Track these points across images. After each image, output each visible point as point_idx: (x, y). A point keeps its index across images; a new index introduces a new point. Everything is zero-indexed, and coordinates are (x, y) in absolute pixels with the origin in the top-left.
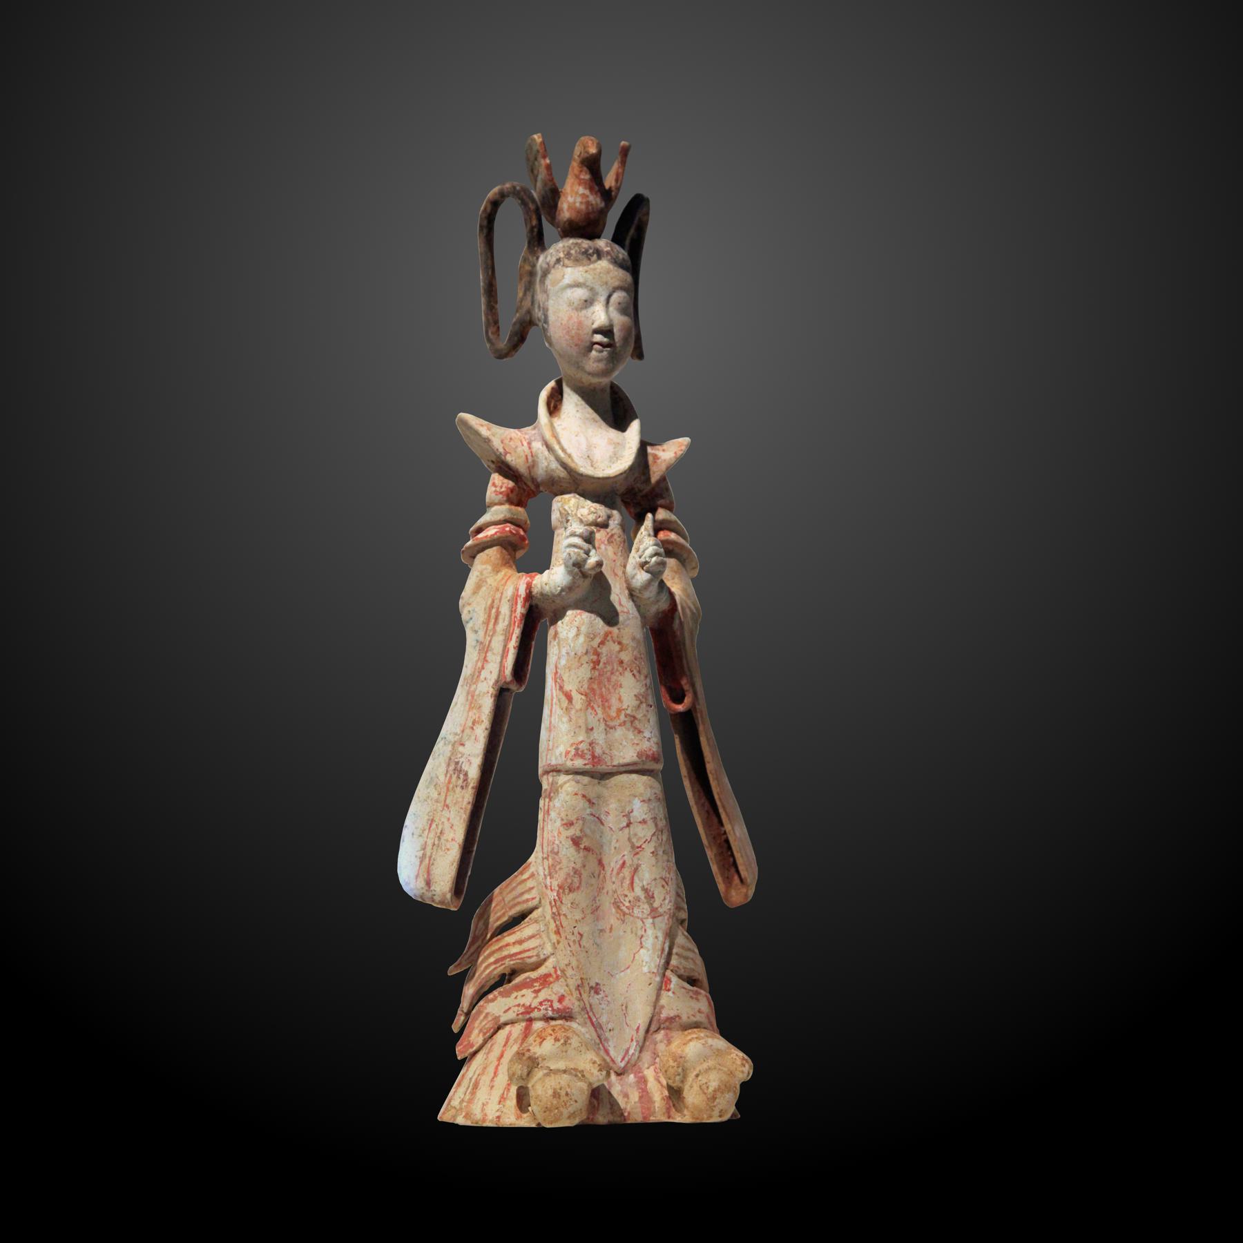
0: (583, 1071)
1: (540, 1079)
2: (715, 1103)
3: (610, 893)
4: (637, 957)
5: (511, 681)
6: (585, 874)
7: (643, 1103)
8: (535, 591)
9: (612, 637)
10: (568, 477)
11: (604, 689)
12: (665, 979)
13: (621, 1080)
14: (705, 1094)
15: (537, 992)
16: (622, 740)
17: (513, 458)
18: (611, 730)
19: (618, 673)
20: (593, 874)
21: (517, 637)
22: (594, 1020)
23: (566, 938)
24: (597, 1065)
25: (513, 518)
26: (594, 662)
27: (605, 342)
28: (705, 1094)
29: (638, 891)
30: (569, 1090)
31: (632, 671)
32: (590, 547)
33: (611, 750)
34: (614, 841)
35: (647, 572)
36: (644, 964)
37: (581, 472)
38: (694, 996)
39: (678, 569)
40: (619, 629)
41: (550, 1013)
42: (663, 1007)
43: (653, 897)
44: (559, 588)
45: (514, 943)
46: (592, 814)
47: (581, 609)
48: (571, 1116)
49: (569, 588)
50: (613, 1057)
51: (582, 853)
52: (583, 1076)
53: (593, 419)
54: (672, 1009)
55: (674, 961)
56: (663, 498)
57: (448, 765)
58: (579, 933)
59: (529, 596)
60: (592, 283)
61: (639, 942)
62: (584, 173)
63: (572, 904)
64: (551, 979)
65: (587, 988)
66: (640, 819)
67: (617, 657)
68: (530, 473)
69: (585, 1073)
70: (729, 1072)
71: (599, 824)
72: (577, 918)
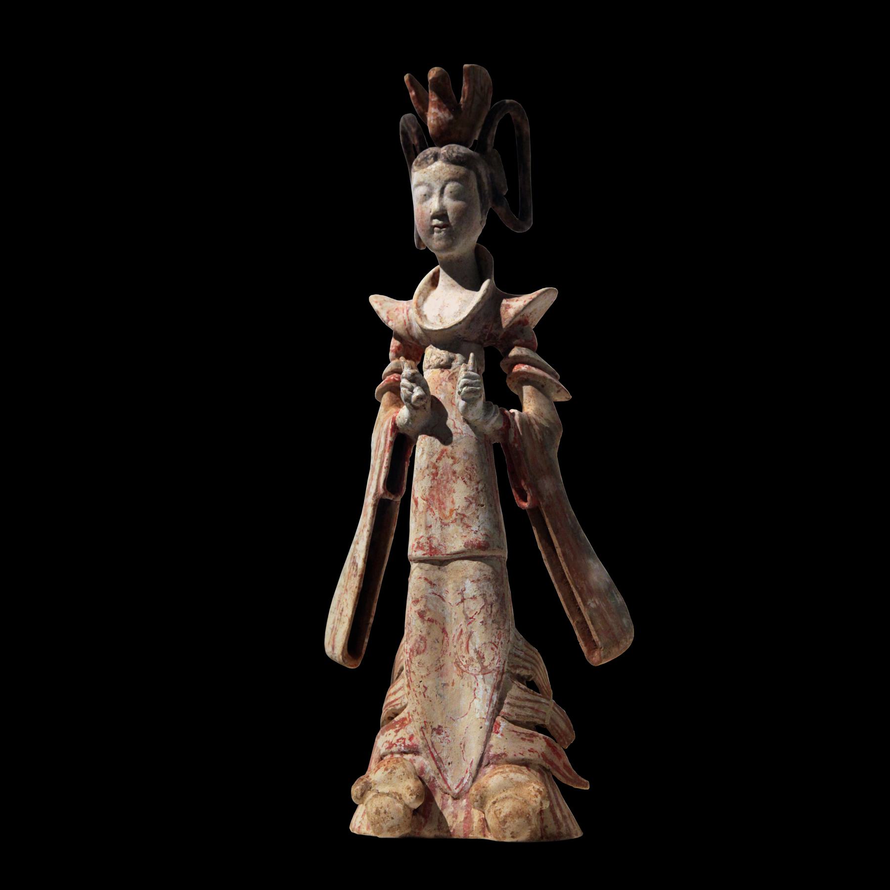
0: (401, 795)
1: (371, 799)
2: (506, 826)
3: (453, 654)
4: (472, 706)
5: (383, 493)
6: (429, 642)
7: (466, 823)
8: (397, 423)
9: (447, 453)
10: (423, 333)
11: (441, 495)
12: (495, 724)
13: (456, 803)
14: (498, 818)
15: (397, 731)
16: (454, 534)
17: (394, 324)
18: (446, 526)
19: (452, 482)
20: (437, 640)
21: (387, 460)
22: (435, 755)
23: (414, 690)
24: (410, 790)
25: (397, 369)
26: (433, 474)
27: (442, 224)
28: (498, 818)
29: (472, 652)
30: (387, 809)
31: (463, 479)
32: (414, 385)
33: (445, 542)
34: (454, 613)
35: (463, 399)
36: (477, 711)
37: (424, 328)
38: (527, 738)
39: (532, 393)
40: (452, 447)
41: (403, 748)
42: (491, 746)
43: (484, 658)
44: (406, 420)
45: (393, 694)
46: (433, 593)
47: (425, 434)
48: (391, 829)
49: (412, 418)
50: (449, 785)
51: (426, 624)
52: (401, 799)
53: (452, 284)
54: (500, 748)
55: (505, 709)
56: (518, 339)
57: (351, 559)
58: (424, 686)
59: (395, 427)
60: (429, 180)
61: (473, 694)
62: (433, 96)
63: (419, 663)
64: (406, 722)
65: (430, 730)
66: (471, 596)
67: (450, 468)
68: (408, 333)
69: (402, 797)
70: (524, 801)
71: (441, 601)
72: (423, 674)
